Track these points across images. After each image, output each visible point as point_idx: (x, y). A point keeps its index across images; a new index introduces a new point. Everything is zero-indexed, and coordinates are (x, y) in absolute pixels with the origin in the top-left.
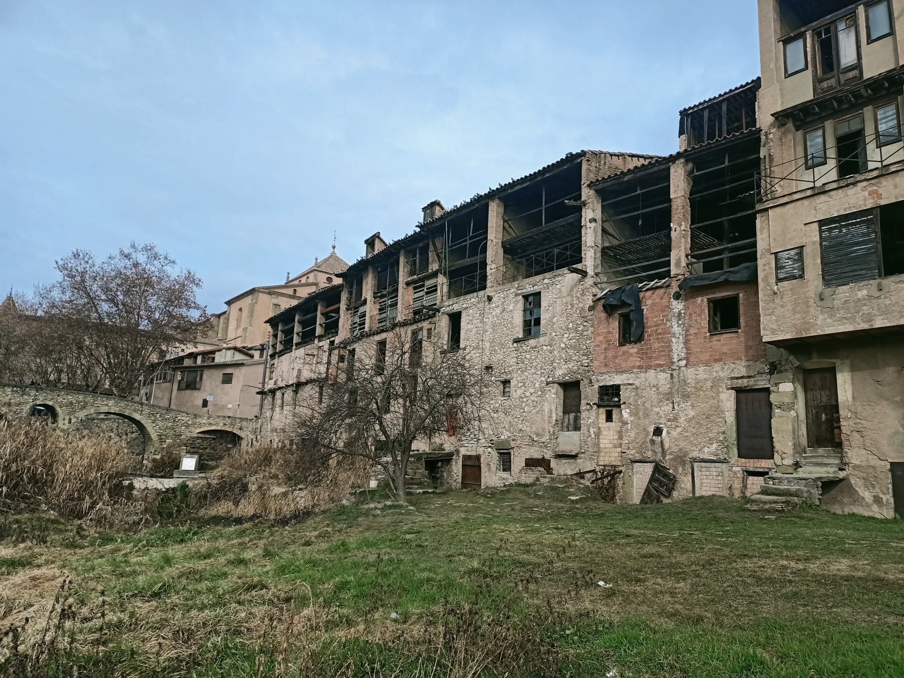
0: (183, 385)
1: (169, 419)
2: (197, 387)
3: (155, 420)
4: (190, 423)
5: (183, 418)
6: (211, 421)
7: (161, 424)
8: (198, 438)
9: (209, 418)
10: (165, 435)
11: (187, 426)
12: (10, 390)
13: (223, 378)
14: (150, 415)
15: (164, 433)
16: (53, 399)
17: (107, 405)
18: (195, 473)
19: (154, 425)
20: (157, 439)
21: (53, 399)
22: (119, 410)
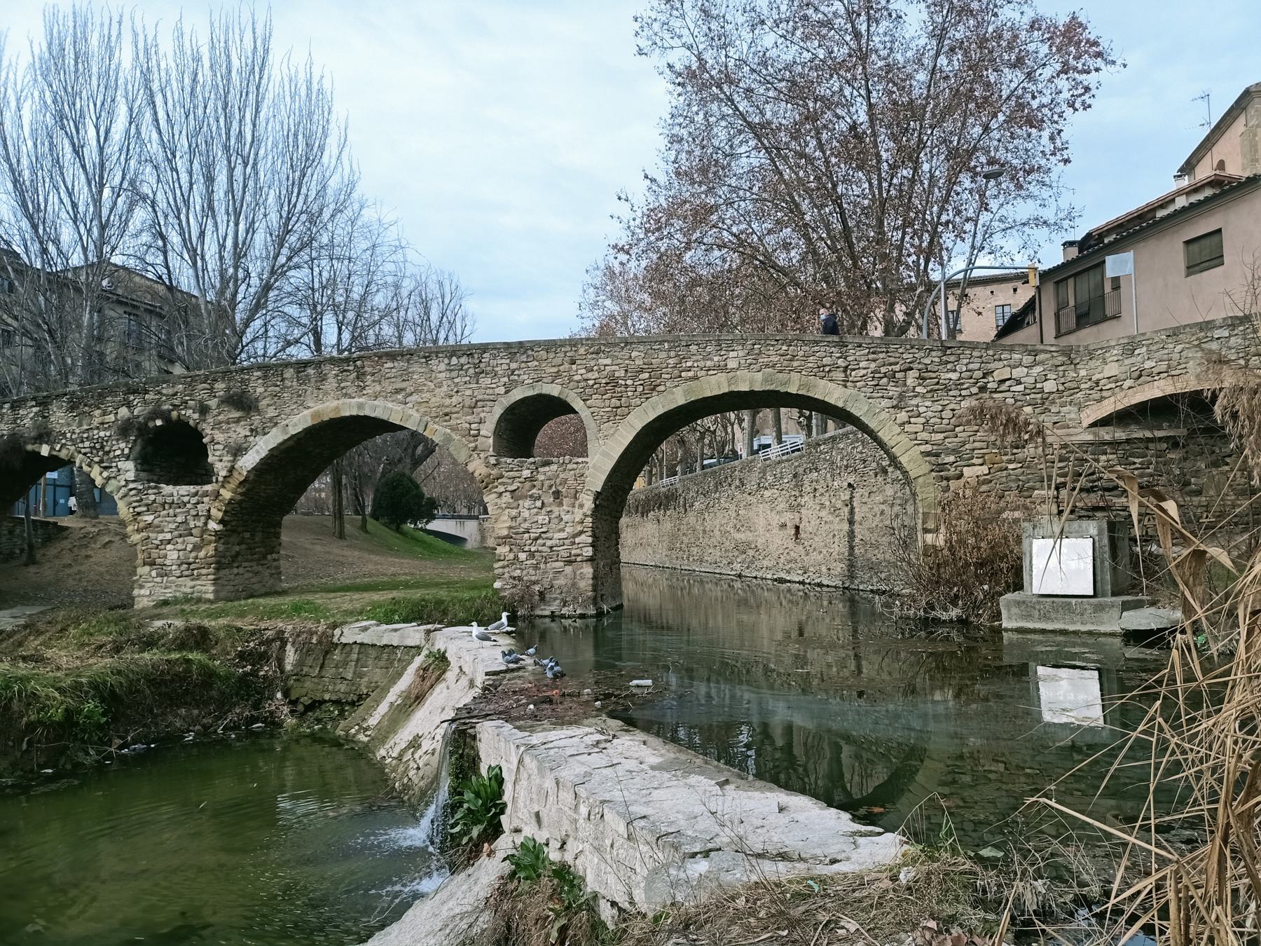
0: (1070, 320)
1: (958, 385)
2: (1109, 313)
3: (901, 397)
4: (1050, 386)
5: (1017, 373)
6: (1141, 358)
7: (927, 407)
8: (1099, 447)
9: (1130, 348)
10: (954, 451)
11: (1043, 403)
12: (442, 367)
13: (1188, 256)
14: (877, 382)
15: (951, 443)
16: (558, 375)
17: (723, 368)
18: (1100, 608)
19: (903, 416)
20: (926, 468)
21: (558, 375)
22: (765, 380)
